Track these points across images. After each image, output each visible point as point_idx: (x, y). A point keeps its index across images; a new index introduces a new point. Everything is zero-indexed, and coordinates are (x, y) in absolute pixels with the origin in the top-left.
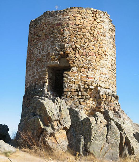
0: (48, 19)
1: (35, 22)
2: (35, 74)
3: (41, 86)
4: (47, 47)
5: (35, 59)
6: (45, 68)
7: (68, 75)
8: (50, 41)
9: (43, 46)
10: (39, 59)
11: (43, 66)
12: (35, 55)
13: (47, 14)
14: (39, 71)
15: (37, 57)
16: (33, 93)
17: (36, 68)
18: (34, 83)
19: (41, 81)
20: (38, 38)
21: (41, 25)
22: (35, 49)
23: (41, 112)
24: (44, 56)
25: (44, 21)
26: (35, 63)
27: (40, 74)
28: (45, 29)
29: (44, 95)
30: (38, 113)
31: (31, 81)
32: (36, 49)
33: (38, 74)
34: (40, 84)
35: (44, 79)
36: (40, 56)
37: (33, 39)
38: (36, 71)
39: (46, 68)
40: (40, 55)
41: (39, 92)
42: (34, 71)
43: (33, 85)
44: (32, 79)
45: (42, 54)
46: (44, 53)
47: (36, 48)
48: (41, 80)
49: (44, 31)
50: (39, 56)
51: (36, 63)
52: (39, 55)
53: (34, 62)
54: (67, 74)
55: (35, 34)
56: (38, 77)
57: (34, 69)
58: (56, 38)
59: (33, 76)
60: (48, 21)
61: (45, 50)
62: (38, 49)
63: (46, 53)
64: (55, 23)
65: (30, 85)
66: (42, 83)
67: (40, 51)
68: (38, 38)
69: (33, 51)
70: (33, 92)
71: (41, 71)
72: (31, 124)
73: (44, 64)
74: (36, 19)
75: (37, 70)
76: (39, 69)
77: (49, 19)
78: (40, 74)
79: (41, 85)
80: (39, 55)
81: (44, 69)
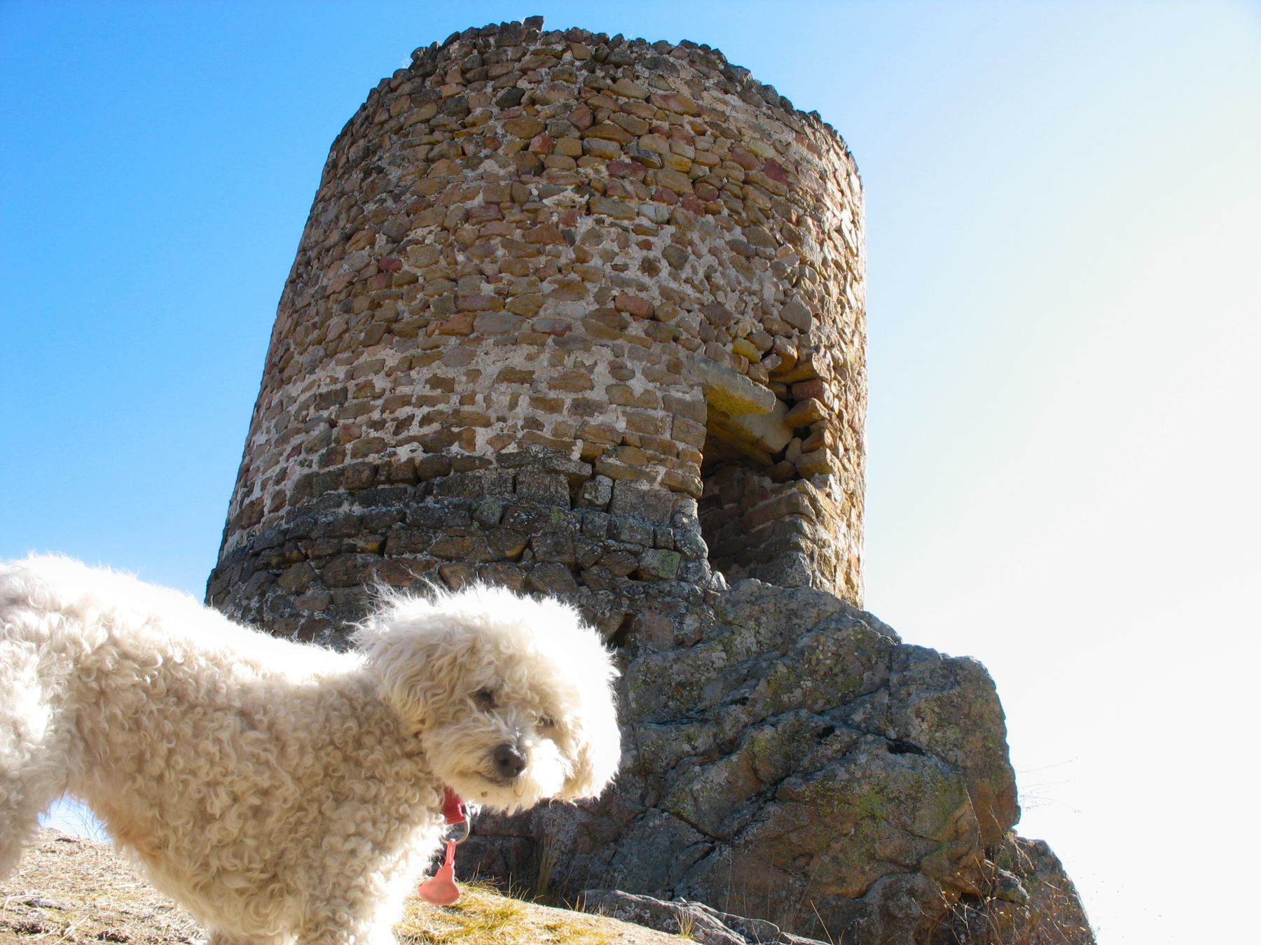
0: (720, 95)
1: (592, 49)
2: (591, 395)
3: (653, 502)
4: (709, 259)
5: (593, 288)
6: (692, 387)
7: (819, 513)
8: (728, 237)
9: (677, 239)
10: (644, 310)
11: (675, 367)
12: (596, 262)
13: (711, 64)
14: (638, 385)
15: (625, 283)
16: (581, 530)
17: (607, 354)
18: (576, 455)
19: (662, 470)
20: (628, 161)
21: (665, 98)
22: (600, 222)
23: (952, 733)
24: (689, 311)
25: (686, 92)
26: (600, 314)
27: (651, 412)
28: (691, 141)
29: (696, 582)
30: (920, 732)
31: (532, 423)
32: (612, 225)
33: (628, 409)
34: (644, 486)
35: (681, 466)
36: (656, 293)
37: (571, 143)
38: (602, 374)
39: (696, 395)
40: (646, 279)
41: (651, 542)
42: (591, 370)
43: (572, 468)
44: (549, 421)
45: (673, 285)
46: (688, 290)
47: (608, 220)
48: (661, 462)
49: (690, 152)
50: (642, 288)
51: (610, 321)
52: (633, 273)
53: (587, 306)
54: (813, 501)
55: (595, 122)
56: (621, 425)
57: (587, 350)
58: (765, 241)
59: (568, 399)
60: (720, 107)
61: (695, 271)
62: (625, 230)
63: (698, 295)
64: (760, 153)
65: (512, 448)
66: (662, 484)
67: (651, 254)
68: (628, 161)
69: (570, 220)
70: (582, 522)
71: (659, 394)
72: (873, 817)
73: (684, 360)
74: (602, 38)
75: (617, 370)
76: (639, 375)
77: (726, 103)
78: (651, 412)
79: (656, 495)
80: (633, 273)
81: (688, 397)
